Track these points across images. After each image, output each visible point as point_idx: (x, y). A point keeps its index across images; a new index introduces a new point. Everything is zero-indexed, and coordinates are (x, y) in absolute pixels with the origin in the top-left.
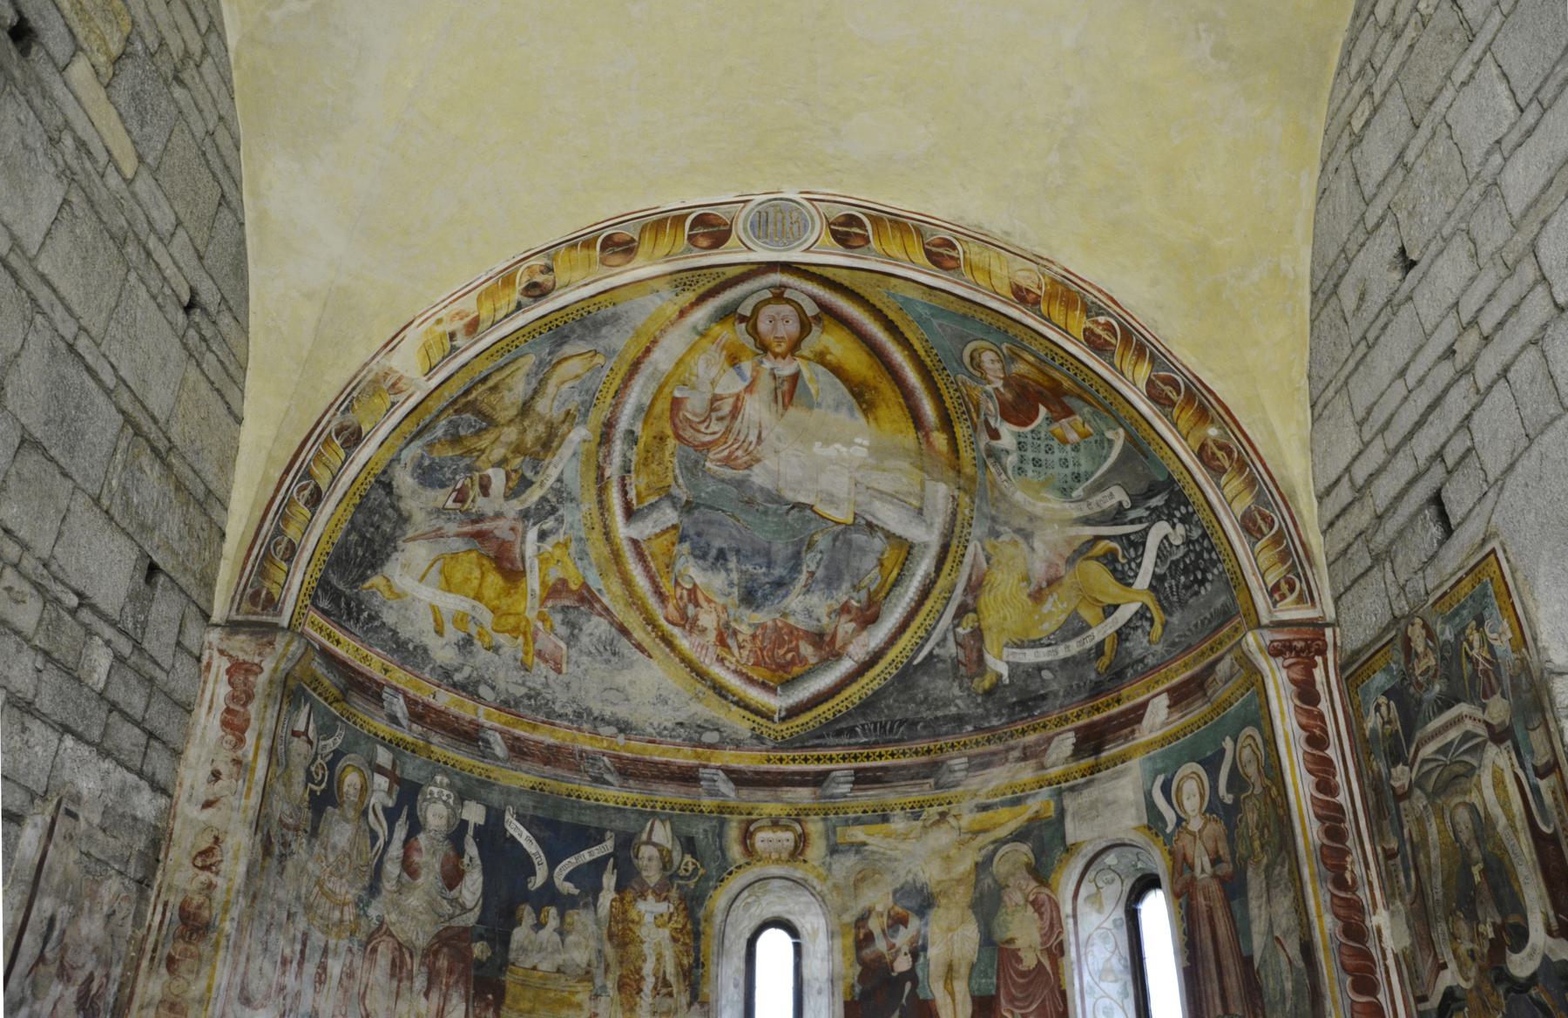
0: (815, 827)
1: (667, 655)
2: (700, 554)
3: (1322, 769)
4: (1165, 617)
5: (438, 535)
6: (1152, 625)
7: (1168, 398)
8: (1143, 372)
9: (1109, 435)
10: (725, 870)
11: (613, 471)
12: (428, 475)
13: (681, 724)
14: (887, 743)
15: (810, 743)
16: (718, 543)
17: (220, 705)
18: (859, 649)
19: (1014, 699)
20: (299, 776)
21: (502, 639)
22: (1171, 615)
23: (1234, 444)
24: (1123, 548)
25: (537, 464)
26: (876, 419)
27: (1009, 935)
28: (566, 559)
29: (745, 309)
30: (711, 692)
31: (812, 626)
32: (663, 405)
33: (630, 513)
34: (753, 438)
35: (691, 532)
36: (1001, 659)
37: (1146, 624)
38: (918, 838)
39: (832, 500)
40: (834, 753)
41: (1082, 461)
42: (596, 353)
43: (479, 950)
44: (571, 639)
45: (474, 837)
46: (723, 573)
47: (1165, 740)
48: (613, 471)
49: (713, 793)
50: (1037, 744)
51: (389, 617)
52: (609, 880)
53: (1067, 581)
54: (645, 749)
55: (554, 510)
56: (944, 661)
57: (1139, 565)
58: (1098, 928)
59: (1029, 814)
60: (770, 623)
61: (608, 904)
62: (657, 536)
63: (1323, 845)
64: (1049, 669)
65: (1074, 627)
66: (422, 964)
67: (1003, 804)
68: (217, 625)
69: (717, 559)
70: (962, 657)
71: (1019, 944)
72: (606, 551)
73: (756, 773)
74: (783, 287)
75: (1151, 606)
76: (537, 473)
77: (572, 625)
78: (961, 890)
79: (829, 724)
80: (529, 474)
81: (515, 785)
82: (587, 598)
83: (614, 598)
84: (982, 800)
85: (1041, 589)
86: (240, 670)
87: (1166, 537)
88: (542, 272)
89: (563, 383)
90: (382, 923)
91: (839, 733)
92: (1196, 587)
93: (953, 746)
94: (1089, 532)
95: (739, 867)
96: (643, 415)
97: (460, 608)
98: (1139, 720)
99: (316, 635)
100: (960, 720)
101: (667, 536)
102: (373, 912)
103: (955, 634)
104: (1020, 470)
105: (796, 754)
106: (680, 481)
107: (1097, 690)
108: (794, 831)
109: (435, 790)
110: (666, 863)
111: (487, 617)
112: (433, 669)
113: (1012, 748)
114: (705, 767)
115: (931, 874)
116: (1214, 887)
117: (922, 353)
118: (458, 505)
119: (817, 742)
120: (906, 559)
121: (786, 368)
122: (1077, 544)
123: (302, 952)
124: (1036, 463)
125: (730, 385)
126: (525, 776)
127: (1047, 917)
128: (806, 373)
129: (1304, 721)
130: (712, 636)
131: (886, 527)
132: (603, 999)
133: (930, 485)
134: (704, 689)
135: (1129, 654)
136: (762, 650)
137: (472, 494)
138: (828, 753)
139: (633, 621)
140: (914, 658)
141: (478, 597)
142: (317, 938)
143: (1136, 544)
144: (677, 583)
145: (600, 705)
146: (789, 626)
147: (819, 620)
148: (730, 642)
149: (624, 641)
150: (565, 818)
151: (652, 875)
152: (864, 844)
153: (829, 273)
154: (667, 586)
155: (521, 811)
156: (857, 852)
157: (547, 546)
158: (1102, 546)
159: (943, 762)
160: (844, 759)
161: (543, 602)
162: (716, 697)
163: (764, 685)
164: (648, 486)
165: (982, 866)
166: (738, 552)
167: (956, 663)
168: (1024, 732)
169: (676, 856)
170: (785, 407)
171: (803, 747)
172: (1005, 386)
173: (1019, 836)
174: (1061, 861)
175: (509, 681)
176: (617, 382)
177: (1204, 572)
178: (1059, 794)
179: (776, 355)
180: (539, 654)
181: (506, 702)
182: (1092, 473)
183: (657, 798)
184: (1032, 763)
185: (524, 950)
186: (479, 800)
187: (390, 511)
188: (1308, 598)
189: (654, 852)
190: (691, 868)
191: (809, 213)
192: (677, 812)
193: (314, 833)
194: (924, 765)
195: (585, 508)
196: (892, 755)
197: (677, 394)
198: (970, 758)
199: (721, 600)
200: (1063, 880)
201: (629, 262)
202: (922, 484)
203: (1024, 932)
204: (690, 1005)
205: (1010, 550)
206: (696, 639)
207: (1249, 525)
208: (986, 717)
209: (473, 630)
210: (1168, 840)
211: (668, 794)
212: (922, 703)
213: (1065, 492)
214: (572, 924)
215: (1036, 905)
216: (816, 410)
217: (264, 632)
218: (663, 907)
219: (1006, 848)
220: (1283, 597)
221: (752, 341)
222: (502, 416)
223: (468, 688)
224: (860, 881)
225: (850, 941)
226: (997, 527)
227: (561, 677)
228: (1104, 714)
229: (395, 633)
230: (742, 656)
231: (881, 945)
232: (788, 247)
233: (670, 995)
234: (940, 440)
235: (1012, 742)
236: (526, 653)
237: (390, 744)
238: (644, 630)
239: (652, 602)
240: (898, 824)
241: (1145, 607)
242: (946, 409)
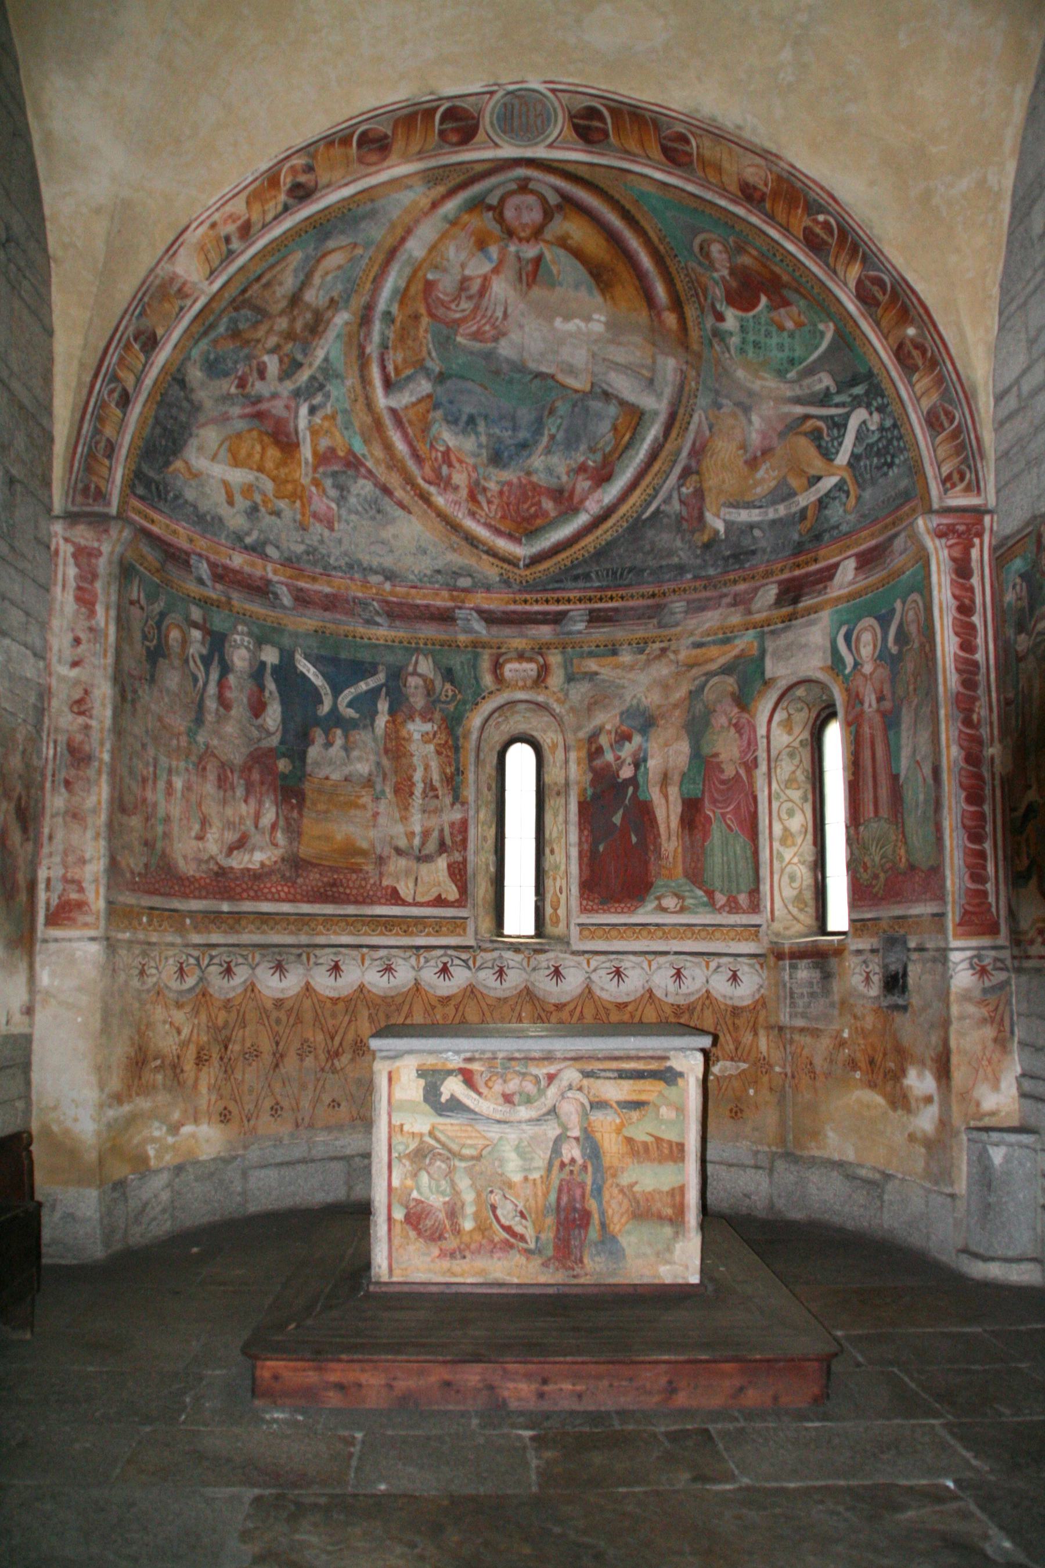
0: (555, 659)
1: (425, 512)
2: (452, 421)
3: (966, 633)
4: (859, 491)
5: (225, 418)
6: (848, 497)
7: (874, 297)
9: (821, 327)
10: (479, 696)
12: (213, 368)
13: (439, 572)
14: (618, 587)
15: (551, 587)
16: (468, 410)
17: (72, 584)
18: (593, 506)
19: (728, 553)
20: (138, 636)
21: (282, 504)
22: (864, 490)
23: (929, 343)
24: (828, 428)
25: (307, 348)
26: (613, 298)
27: (715, 750)
28: (333, 429)
29: (493, 200)
30: (463, 543)
31: (553, 482)
32: (417, 287)
33: (388, 385)
34: (499, 314)
35: (444, 400)
36: (718, 516)
37: (843, 496)
38: (642, 670)
39: (571, 371)
40: (571, 595)
41: (797, 347)
42: (355, 245)
43: (283, 765)
44: (341, 500)
45: (272, 674)
46: (473, 437)
47: (851, 597)
48: (372, 349)
49: (469, 631)
50: (746, 592)
51: (190, 495)
52: (383, 706)
53: (779, 452)
54: (408, 594)
55: (321, 387)
56: (669, 516)
57: (840, 444)
58: (788, 746)
59: (735, 652)
60: (515, 480)
61: (383, 725)
62: (414, 405)
63: (958, 693)
64: (760, 528)
65: (783, 494)
66: (240, 777)
67: (714, 643)
68: (58, 517)
69: (468, 423)
70: (684, 513)
71: (723, 757)
72: (369, 420)
73: (504, 612)
74: (528, 180)
75: (848, 480)
76: (306, 355)
77: (342, 488)
78: (677, 713)
79: (568, 570)
80: (299, 357)
81: (301, 630)
82: (353, 463)
83: (377, 462)
84: (698, 639)
85: (755, 458)
86: (83, 555)
87: (864, 422)
89: (327, 273)
90: (207, 746)
91: (576, 578)
92: (885, 469)
93: (674, 591)
94: (799, 410)
95: (491, 693)
96: (398, 297)
97: (246, 481)
98: (831, 577)
99: (137, 518)
100: (681, 569)
101: (423, 405)
102: (200, 739)
103: (679, 494)
104: (742, 351)
105: (539, 596)
106: (434, 354)
107: (799, 549)
108: (537, 662)
109: (238, 638)
110: (429, 690)
111: (269, 486)
112: (228, 536)
113: (725, 595)
114: (460, 608)
115: (652, 699)
116: (877, 719)
117: (656, 240)
118: (240, 390)
119: (556, 585)
120: (638, 424)
121: (530, 251)
122: (789, 420)
123: (155, 774)
124: (756, 345)
125: (478, 267)
126: (309, 621)
127: (745, 737)
128: (548, 256)
129: (957, 592)
130: (464, 493)
131: (620, 395)
132: (383, 801)
133: (660, 359)
134: (458, 540)
135: (827, 519)
136: (508, 505)
137: (251, 380)
138: (566, 595)
139: (394, 481)
140: (643, 513)
141: (261, 469)
142: (163, 760)
143: (839, 425)
144: (432, 446)
145: (368, 557)
146: (531, 482)
147: (559, 478)
148: (481, 498)
149: (387, 499)
150: (343, 655)
151: (419, 701)
152: (596, 674)
154: (423, 449)
155: (308, 651)
156: (591, 680)
157: (317, 420)
158: (810, 424)
159: (665, 605)
160: (580, 600)
161: (315, 469)
162: (469, 547)
163: (510, 537)
164: (405, 360)
165: (694, 694)
166: (486, 417)
167: (680, 519)
168: (735, 582)
169: (438, 683)
170: (529, 286)
171: (545, 590)
172: (731, 274)
173: (727, 670)
174: (759, 692)
176: (375, 269)
177: (893, 457)
178: (762, 637)
179: (520, 240)
180: (315, 515)
181: (289, 559)
182: (805, 359)
183: (422, 636)
184: (741, 608)
185: (317, 764)
186: (273, 644)
187: (185, 404)
189: (420, 682)
190: (450, 694)
191: (552, 104)
192: (438, 647)
193: (152, 680)
194: (649, 607)
195: (349, 383)
196: (622, 598)
197: (430, 277)
198: (688, 602)
199: (471, 461)
200: (760, 708)
201: (384, 159)
202: (653, 357)
204: (453, 804)
205: (730, 421)
206: (451, 496)
207: (933, 422)
208: (703, 567)
209: (258, 498)
210: (846, 678)
211: (429, 631)
212: (649, 553)
213: (781, 373)
214: (355, 742)
215: (738, 727)
216: (558, 289)
217: (100, 521)
218: (428, 727)
219: (716, 679)
220: (954, 486)
221: (498, 227)
222: (276, 308)
223: (257, 550)
224: (593, 705)
225: (583, 754)
226: (720, 400)
227: (334, 534)
228: (803, 571)
229: (195, 507)
230: (490, 510)
231: (609, 757)
233: (437, 797)
234: (671, 319)
235: (725, 590)
236: (303, 515)
238: (404, 489)
239: (411, 465)
240: (626, 657)
241: (842, 482)
242: (677, 292)
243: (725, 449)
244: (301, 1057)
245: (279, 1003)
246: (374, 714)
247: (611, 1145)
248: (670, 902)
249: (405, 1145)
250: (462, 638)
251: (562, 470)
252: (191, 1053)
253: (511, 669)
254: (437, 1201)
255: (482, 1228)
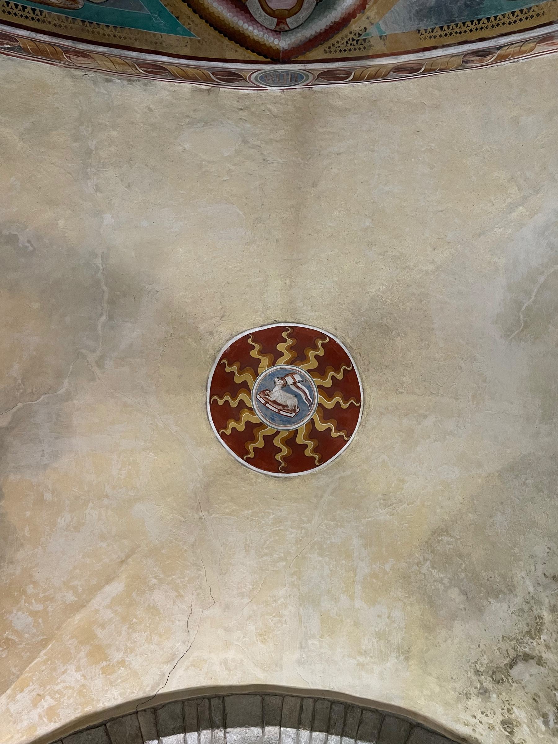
74: (278, 32)
88: (472, 60)
153: (242, 53)
232: (273, 72)
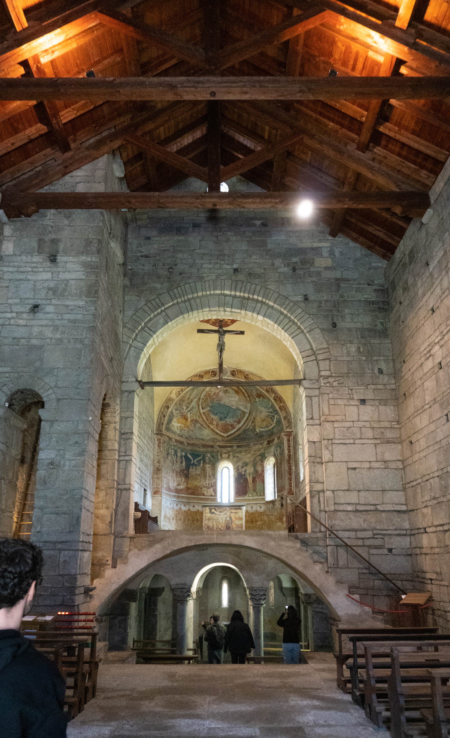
0: (231, 454)
8: (273, 395)
11: (200, 403)
25: (190, 404)
33: (202, 408)
39: (232, 405)
48: (200, 403)
52: (202, 462)
77: (195, 425)
82: (197, 421)
86: (159, 440)
100: (252, 438)
107: (270, 436)
110: (209, 459)
111: (183, 426)
115: (248, 460)
139: (203, 424)
143: (274, 417)
151: (208, 461)
173: (260, 455)
175: (186, 434)
188: (291, 428)
203: (259, 469)
207: (285, 418)
211: (210, 449)
213: (265, 408)
215: (261, 465)
217: (162, 435)
224: (238, 461)
234: (248, 399)
237: (173, 446)
239: (206, 421)
240: (243, 453)
243: (258, 419)
244: (188, 521)
245: (185, 511)
246: (200, 463)
247: (233, 518)
248: (250, 495)
249: (207, 518)
250: (215, 450)
251: (232, 421)
252: (171, 518)
253: (224, 455)
254: (211, 525)
255: (217, 529)
